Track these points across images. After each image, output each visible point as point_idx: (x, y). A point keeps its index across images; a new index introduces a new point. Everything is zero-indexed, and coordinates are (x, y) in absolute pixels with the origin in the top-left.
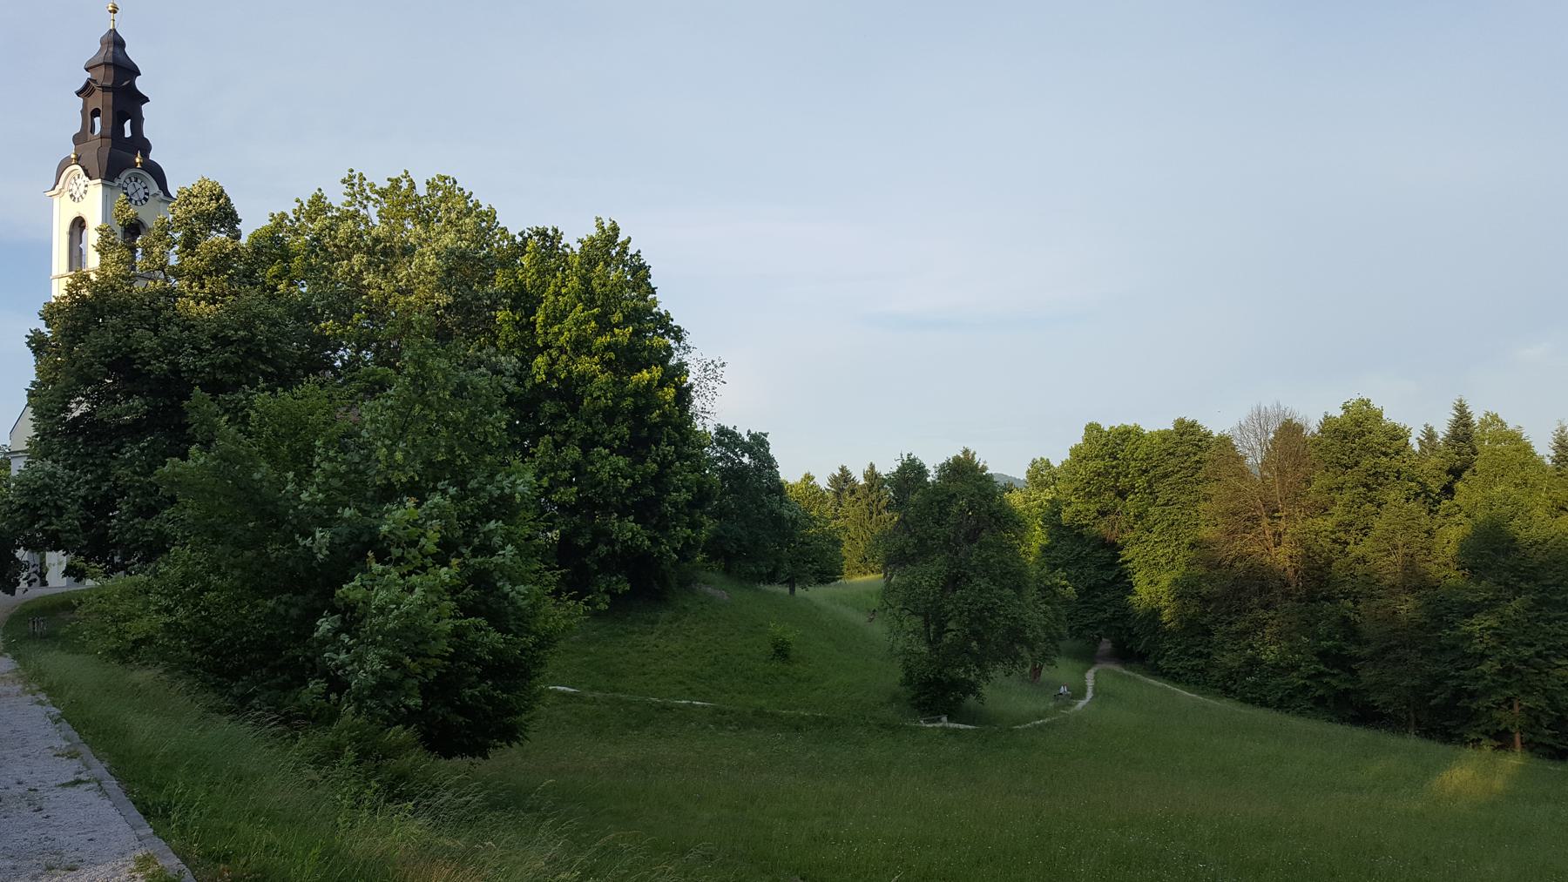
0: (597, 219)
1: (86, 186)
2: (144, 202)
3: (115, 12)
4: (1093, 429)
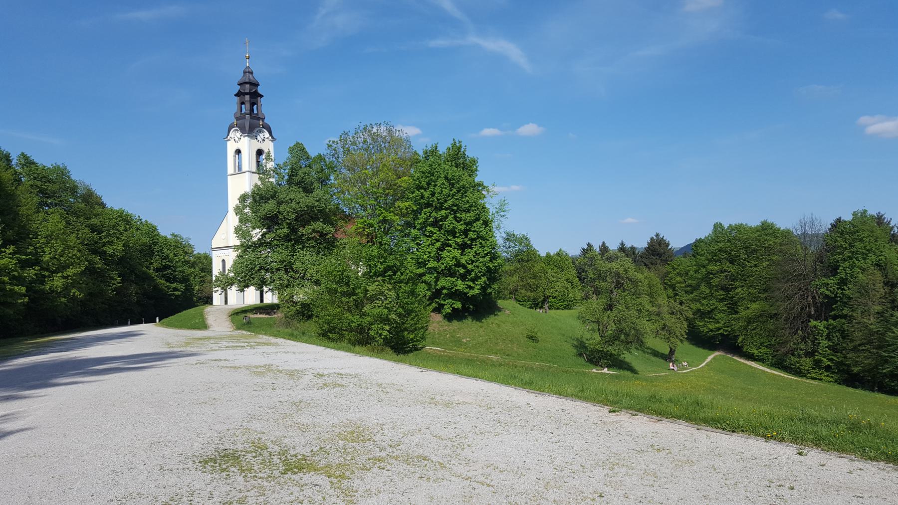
0: (454, 140)
1: (241, 136)
3: (248, 58)
4: (718, 227)
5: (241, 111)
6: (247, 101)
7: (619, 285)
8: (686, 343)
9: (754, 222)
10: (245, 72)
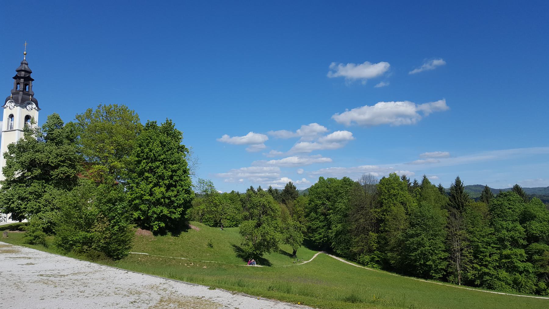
2: (31, 110)
4: (321, 179)
5: (17, 89)
6: (22, 82)
7: (265, 213)
8: (302, 247)
9: (340, 178)
10: (22, 64)
